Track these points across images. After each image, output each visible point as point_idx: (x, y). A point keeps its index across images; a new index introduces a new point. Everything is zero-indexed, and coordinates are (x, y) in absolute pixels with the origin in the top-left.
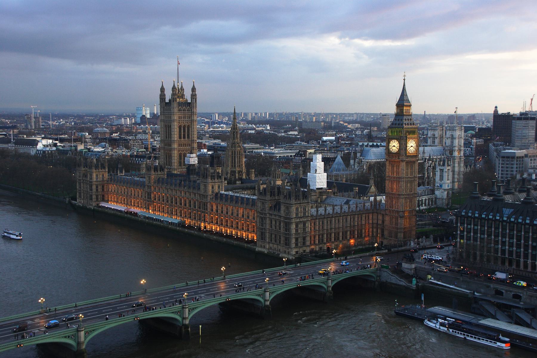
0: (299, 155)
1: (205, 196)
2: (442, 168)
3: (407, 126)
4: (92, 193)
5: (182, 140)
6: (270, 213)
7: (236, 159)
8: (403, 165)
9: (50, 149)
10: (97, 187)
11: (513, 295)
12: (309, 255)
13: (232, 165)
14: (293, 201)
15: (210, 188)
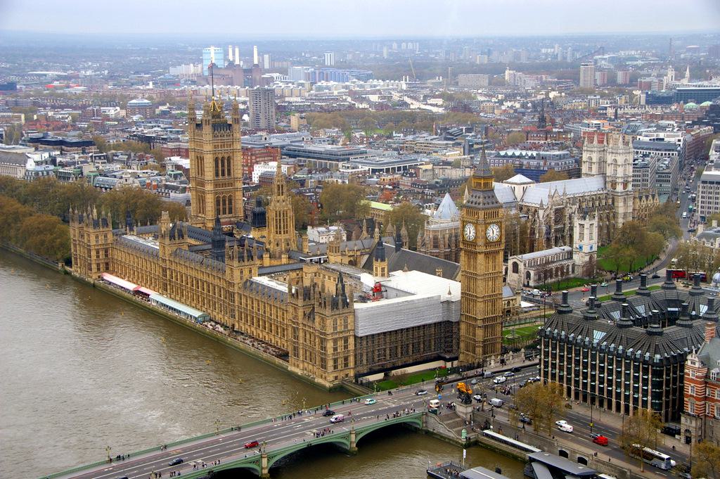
0: (408, 175)
1: (231, 284)
2: (582, 222)
3: (487, 206)
4: (91, 260)
5: (221, 177)
6: (304, 323)
7: (282, 222)
8: (481, 258)
9: (46, 169)
10: (98, 252)
11: (579, 458)
12: (354, 381)
13: (277, 233)
14: (328, 312)
15: (237, 273)
